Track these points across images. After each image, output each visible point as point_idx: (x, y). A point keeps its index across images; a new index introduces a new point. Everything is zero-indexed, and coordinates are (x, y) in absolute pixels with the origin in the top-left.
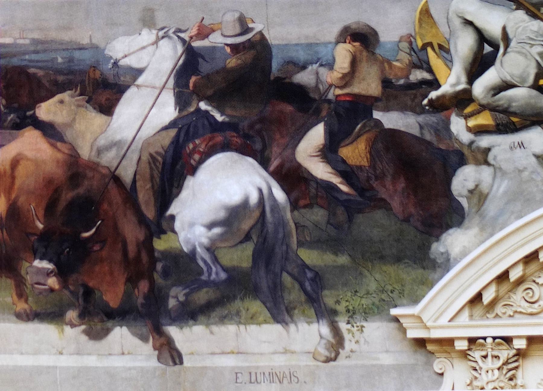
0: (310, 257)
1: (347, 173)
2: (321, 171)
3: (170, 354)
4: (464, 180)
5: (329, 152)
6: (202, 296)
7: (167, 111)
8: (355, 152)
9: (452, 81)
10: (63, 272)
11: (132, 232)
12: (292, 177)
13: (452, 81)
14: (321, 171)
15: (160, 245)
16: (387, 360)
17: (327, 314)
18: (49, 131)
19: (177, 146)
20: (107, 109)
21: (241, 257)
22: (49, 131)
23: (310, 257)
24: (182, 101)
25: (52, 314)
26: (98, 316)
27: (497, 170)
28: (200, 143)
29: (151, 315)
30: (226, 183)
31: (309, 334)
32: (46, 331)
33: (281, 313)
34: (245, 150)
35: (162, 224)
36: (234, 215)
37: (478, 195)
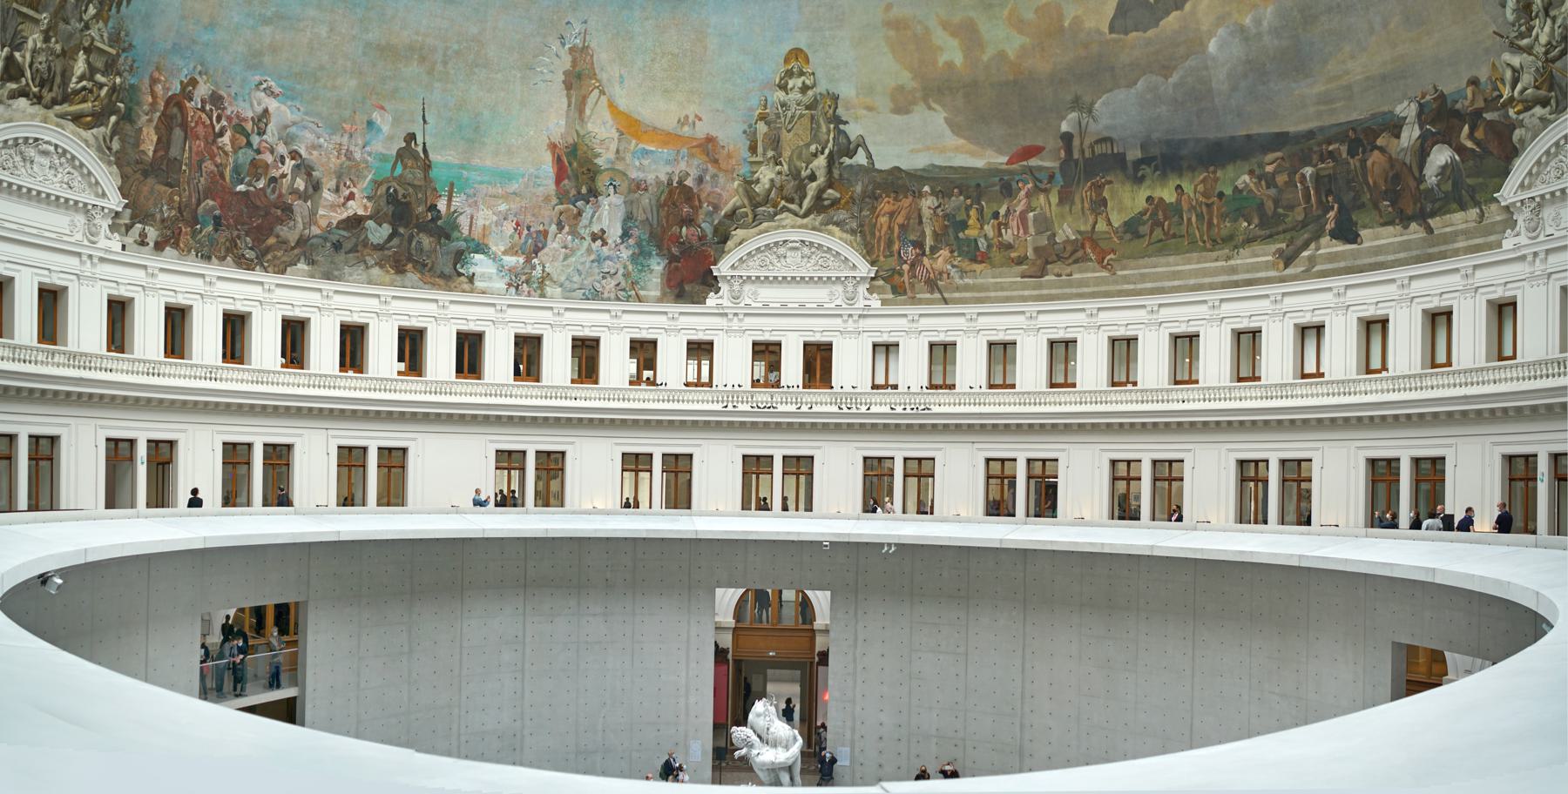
0: (1470, 181)
1: (1478, 143)
2: (1469, 144)
3: (1430, 230)
4: (1517, 134)
5: (1471, 136)
6: (1437, 205)
7: (1417, 133)
8: (1479, 134)
9: (1506, 93)
10: (1392, 205)
11: (1412, 184)
12: (1460, 149)
13: (1506, 93)
14: (1469, 144)
15: (1422, 187)
16: (1498, 218)
17: (1477, 204)
18: (1382, 150)
19: (1422, 145)
20: (1398, 136)
21: (1448, 187)
22: (1382, 150)
23: (1470, 181)
24: (1421, 128)
25: (1390, 223)
26: (1404, 220)
27: (1528, 129)
28: (1429, 143)
29: (1422, 217)
30: (1441, 156)
31: (1473, 213)
32: (1390, 228)
33: (1463, 208)
34: (1444, 142)
35: (1421, 179)
36: (1444, 168)
37: (1522, 141)
